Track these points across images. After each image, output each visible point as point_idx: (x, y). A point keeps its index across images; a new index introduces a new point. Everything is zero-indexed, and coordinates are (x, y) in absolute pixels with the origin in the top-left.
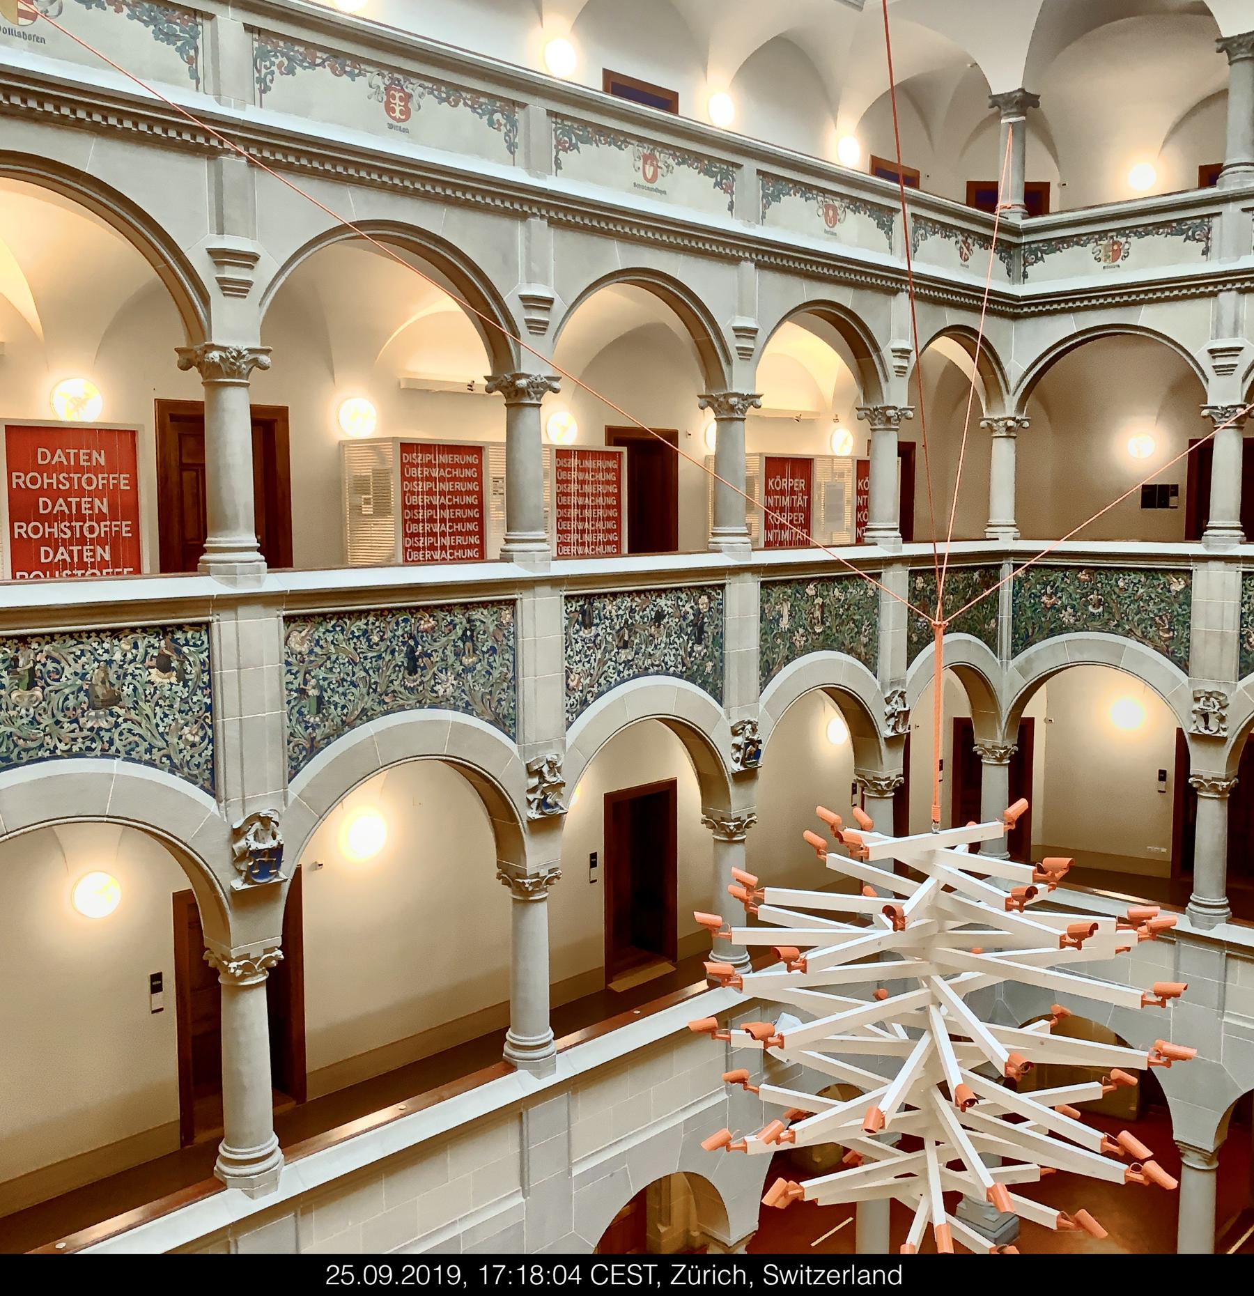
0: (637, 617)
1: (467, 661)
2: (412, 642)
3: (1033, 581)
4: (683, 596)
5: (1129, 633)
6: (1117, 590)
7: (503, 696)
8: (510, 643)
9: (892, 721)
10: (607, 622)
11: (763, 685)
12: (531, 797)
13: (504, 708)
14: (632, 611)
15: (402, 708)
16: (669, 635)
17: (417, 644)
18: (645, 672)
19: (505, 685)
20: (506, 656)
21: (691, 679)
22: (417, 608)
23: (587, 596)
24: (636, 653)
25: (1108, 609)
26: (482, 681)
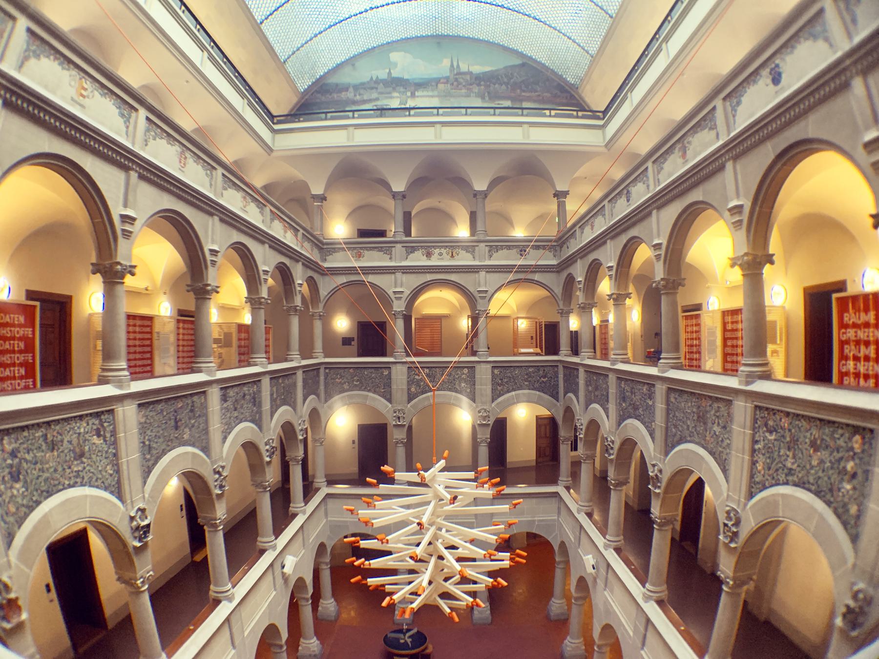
5: (369, 391)
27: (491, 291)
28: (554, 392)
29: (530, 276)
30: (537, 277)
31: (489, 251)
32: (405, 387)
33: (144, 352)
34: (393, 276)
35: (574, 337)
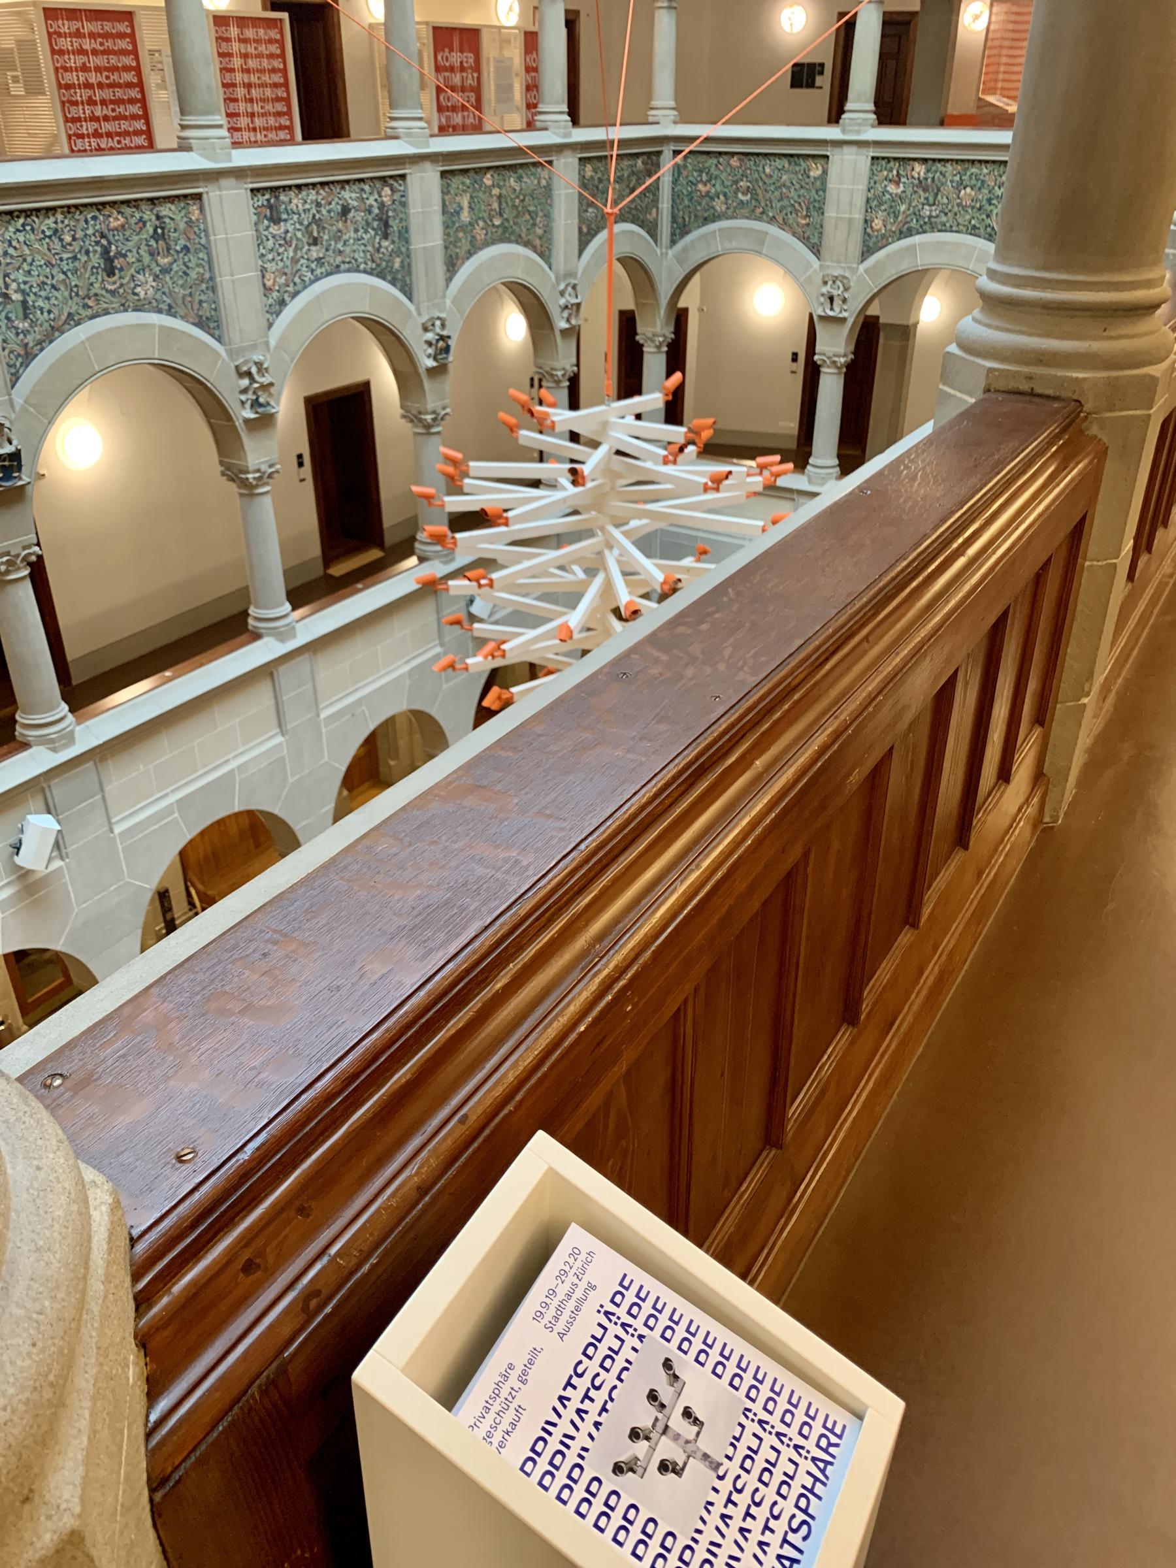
0: (324, 212)
1: (164, 261)
2: (104, 242)
4: (367, 188)
5: (772, 220)
6: (763, 176)
7: (203, 298)
8: (203, 241)
9: (565, 314)
10: (295, 217)
11: (449, 280)
12: (243, 398)
13: (206, 311)
14: (318, 205)
15: (106, 312)
16: (356, 231)
17: (110, 243)
18: (337, 270)
19: (204, 286)
20: (201, 255)
21: (381, 275)
22: (104, 204)
23: (273, 190)
24: (327, 250)
25: (755, 196)
26: (180, 282)
32: (858, 216)
33: (119, 102)
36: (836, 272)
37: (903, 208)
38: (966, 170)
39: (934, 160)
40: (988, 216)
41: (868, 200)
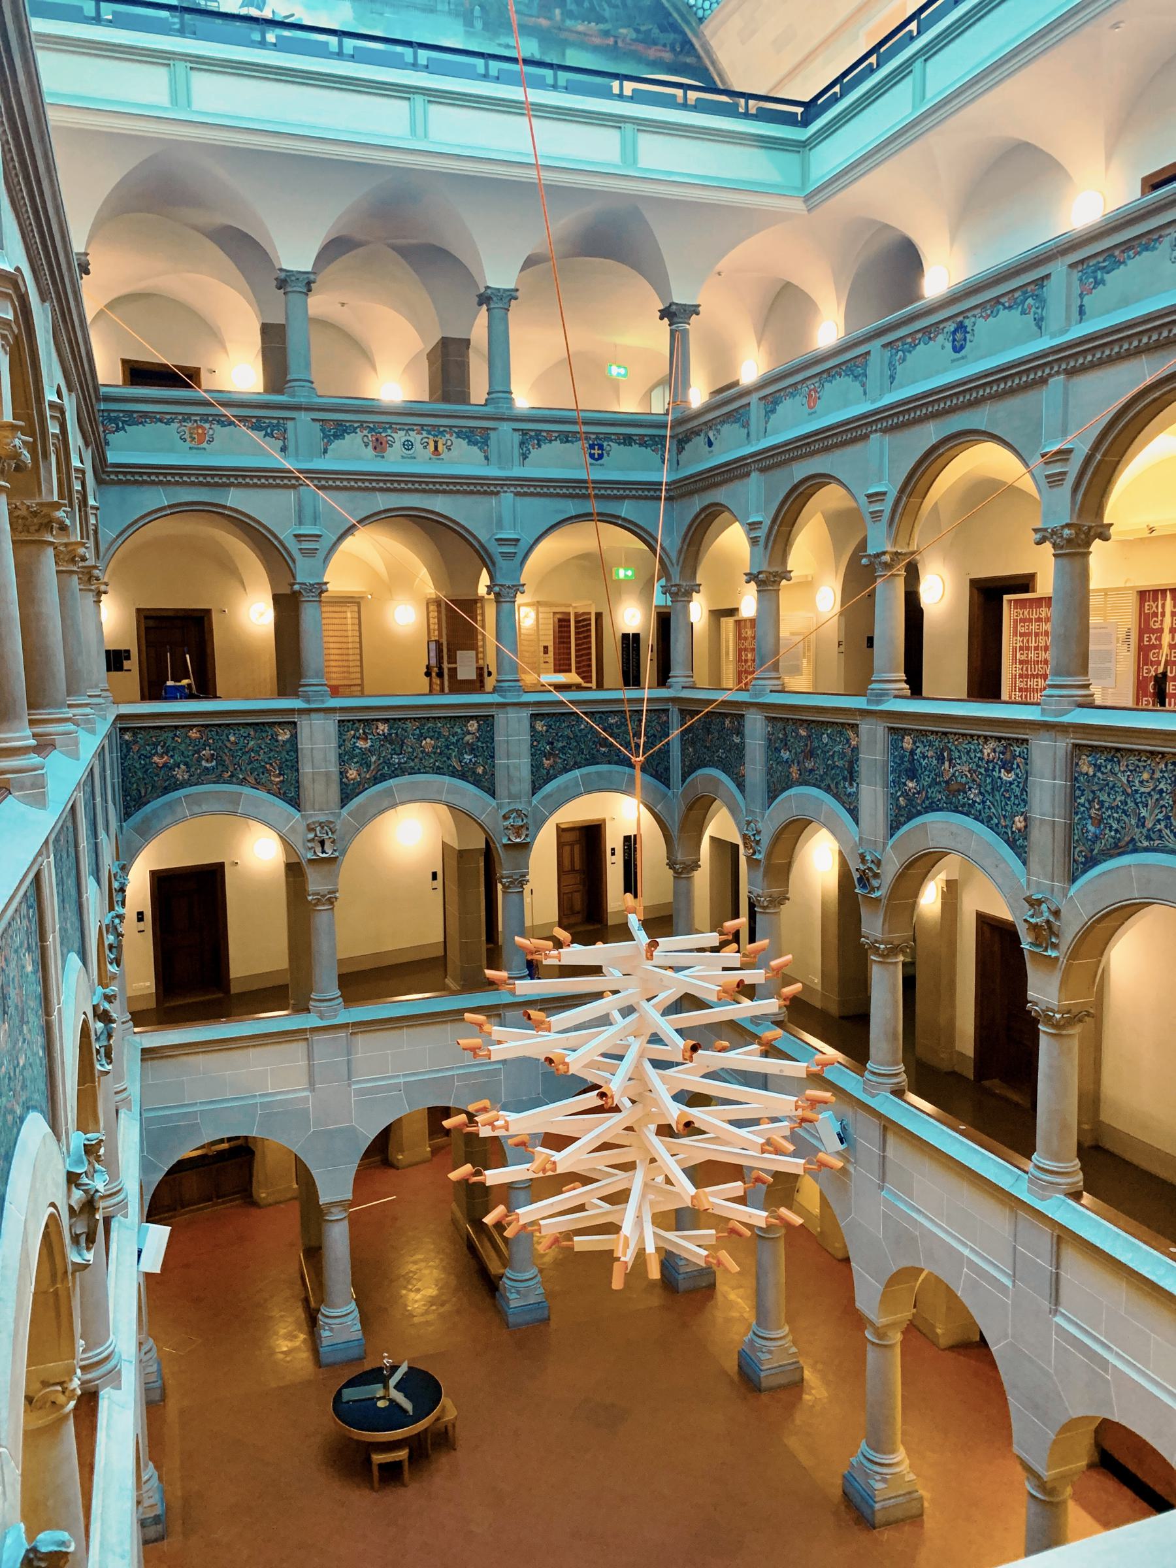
3: (142, 742)
5: (241, 782)
6: (228, 745)
25: (221, 763)
27: (527, 539)
28: (661, 769)
29: (610, 508)
30: (625, 509)
31: (522, 444)
32: (334, 769)
34: (292, 493)
35: (631, 643)
36: (323, 819)
37: (373, 759)
38: (424, 725)
39: (394, 719)
40: (449, 759)
41: (340, 755)
